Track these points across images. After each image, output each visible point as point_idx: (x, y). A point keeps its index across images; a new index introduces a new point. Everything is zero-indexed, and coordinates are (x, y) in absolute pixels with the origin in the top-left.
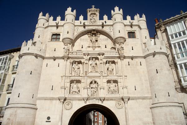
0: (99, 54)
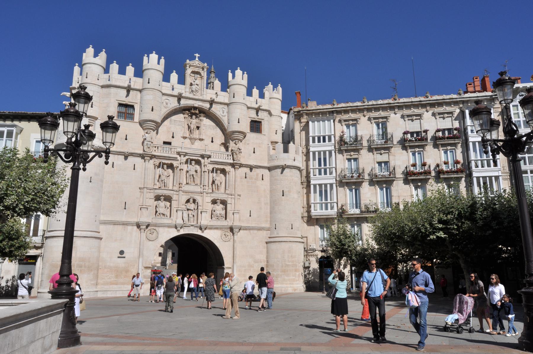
0: (203, 156)
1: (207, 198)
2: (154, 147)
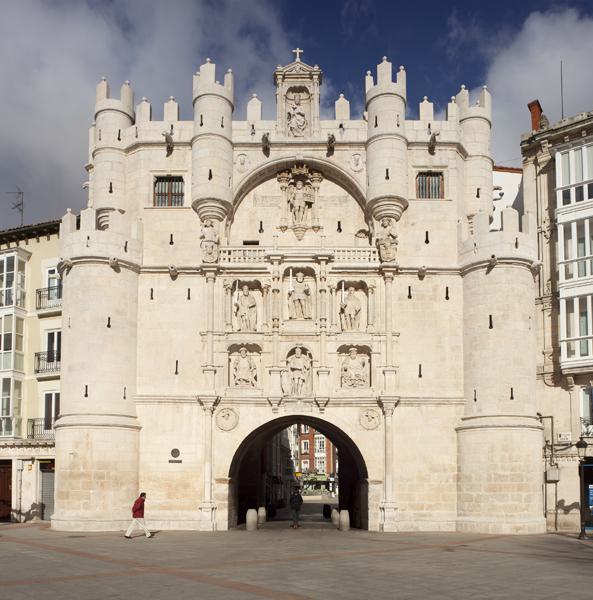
0: (316, 259)
1: (328, 344)
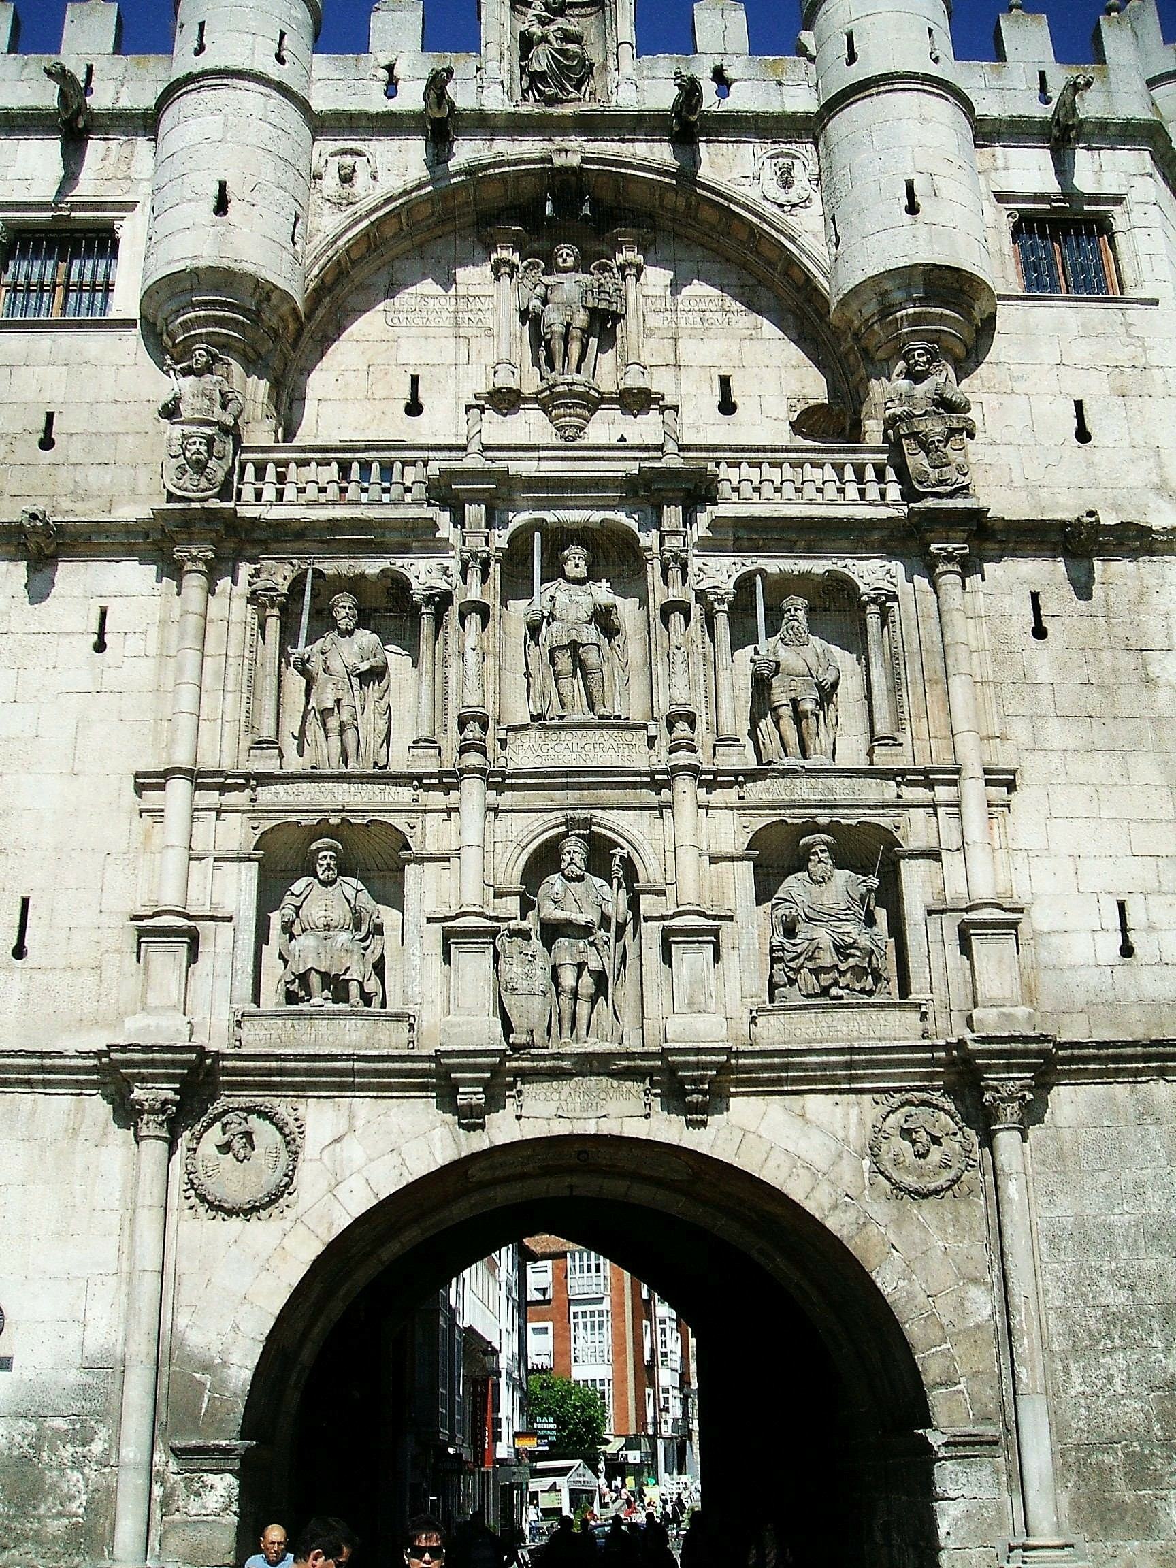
2: (250, 469)
